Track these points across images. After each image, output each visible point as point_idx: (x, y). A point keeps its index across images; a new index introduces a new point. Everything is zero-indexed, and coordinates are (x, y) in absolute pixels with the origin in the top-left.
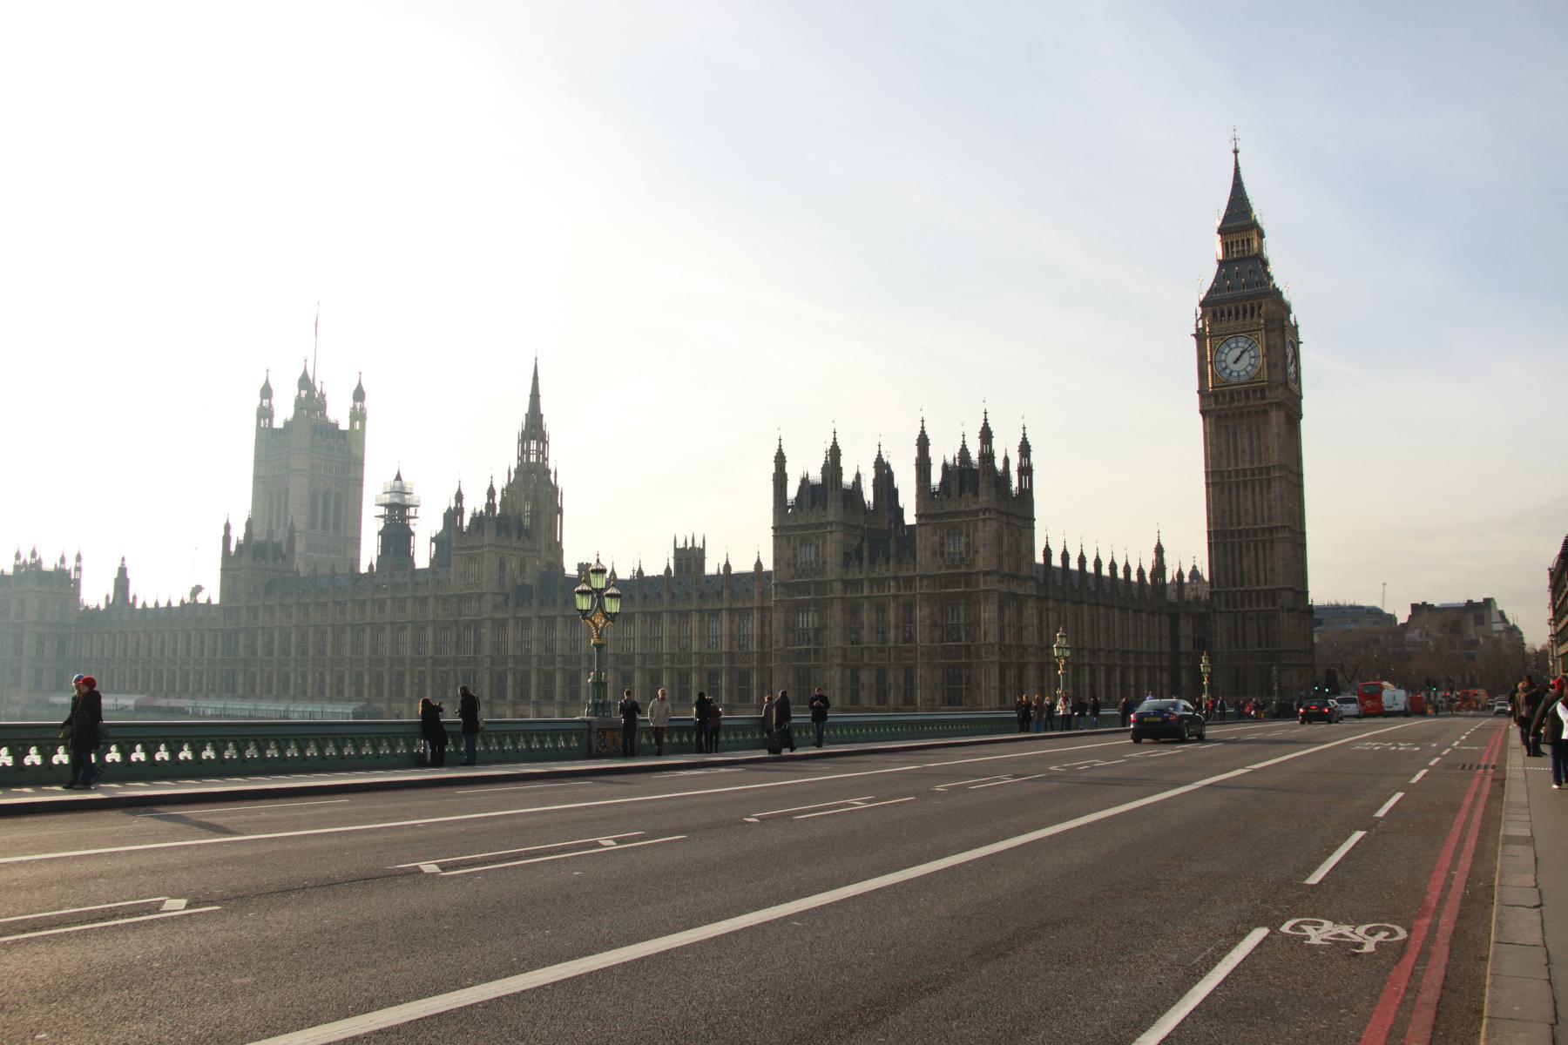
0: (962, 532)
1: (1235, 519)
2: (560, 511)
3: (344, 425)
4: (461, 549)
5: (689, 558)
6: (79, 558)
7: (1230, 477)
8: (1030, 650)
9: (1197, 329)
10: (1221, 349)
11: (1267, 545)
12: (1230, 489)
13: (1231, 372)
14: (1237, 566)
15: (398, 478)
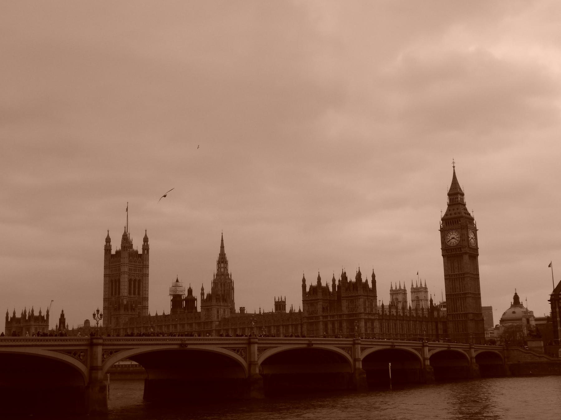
0: (354, 302)
1: (454, 290)
2: (233, 289)
3: (140, 252)
4: (204, 306)
5: (280, 305)
6: (48, 312)
7: (452, 276)
8: (377, 335)
9: (441, 228)
10: (448, 235)
11: (464, 298)
12: (452, 280)
13: (451, 242)
14: (455, 305)
15: (177, 281)
